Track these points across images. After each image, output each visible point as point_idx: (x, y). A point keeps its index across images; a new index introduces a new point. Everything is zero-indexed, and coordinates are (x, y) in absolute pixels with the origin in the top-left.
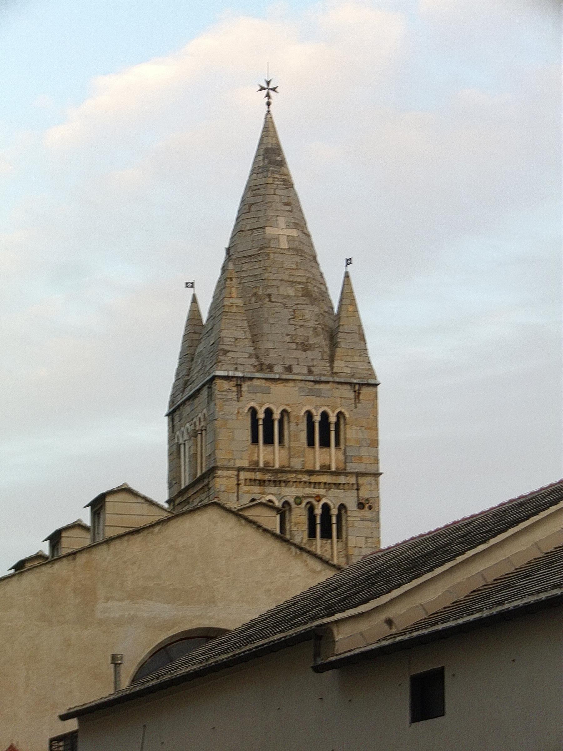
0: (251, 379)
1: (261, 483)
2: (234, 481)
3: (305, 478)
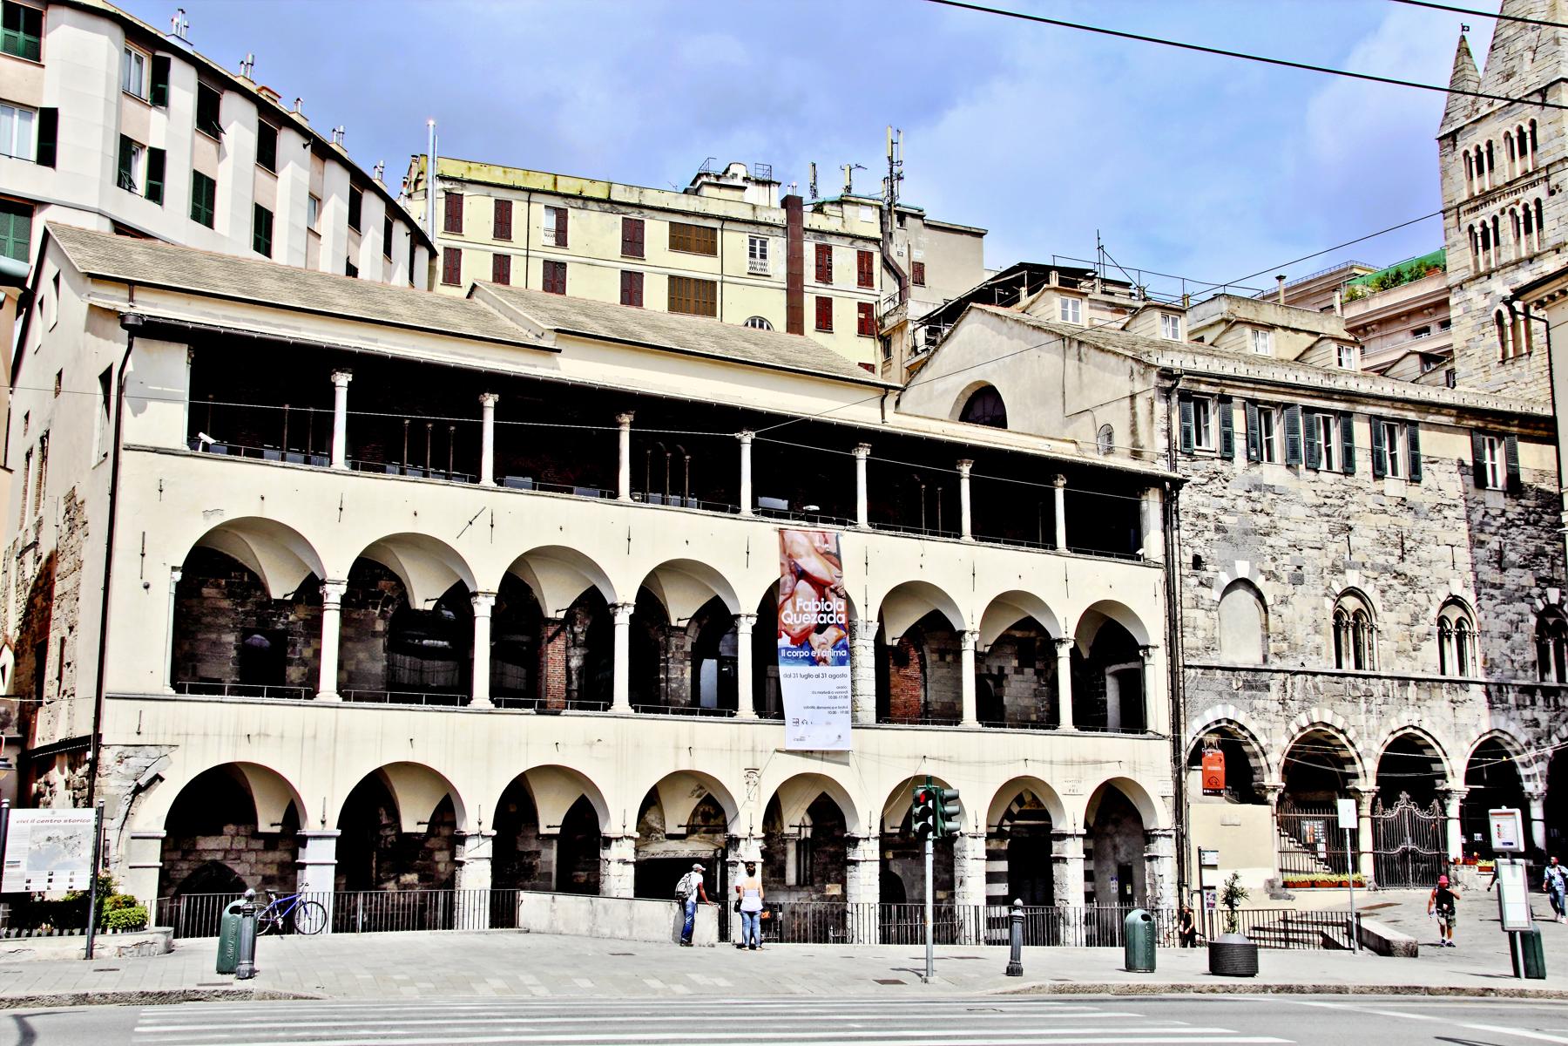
0: (1462, 128)
1: (1476, 209)
2: (1455, 217)
3: (1507, 190)
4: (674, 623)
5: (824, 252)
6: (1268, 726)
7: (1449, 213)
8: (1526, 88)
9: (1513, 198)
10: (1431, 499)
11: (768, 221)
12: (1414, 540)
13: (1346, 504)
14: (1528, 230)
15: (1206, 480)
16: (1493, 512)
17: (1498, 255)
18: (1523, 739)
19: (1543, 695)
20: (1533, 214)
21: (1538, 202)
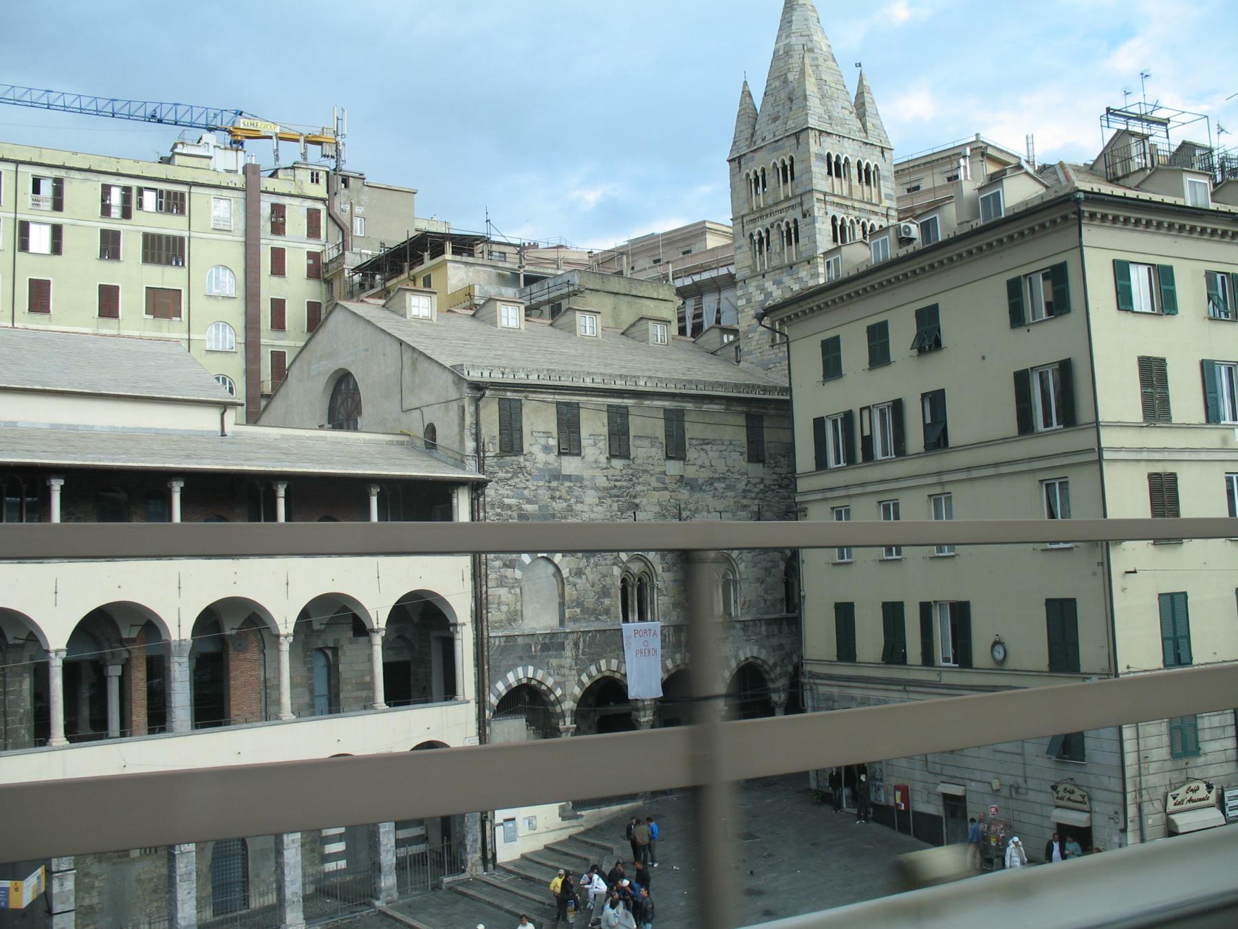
0: (745, 155)
1: (753, 221)
2: (741, 225)
3: (774, 209)
4: (11, 642)
5: (278, 210)
6: (563, 679)
7: (737, 222)
8: (786, 131)
9: (778, 216)
10: (704, 475)
11: (230, 185)
12: (690, 510)
13: (633, 485)
14: (790, 243)
15: (510, 475)
16: (753, 481)
17: (769, 260)
18: (771, 662)
19: (787, 625)
20: (793, 231)
21: (795, 221)
